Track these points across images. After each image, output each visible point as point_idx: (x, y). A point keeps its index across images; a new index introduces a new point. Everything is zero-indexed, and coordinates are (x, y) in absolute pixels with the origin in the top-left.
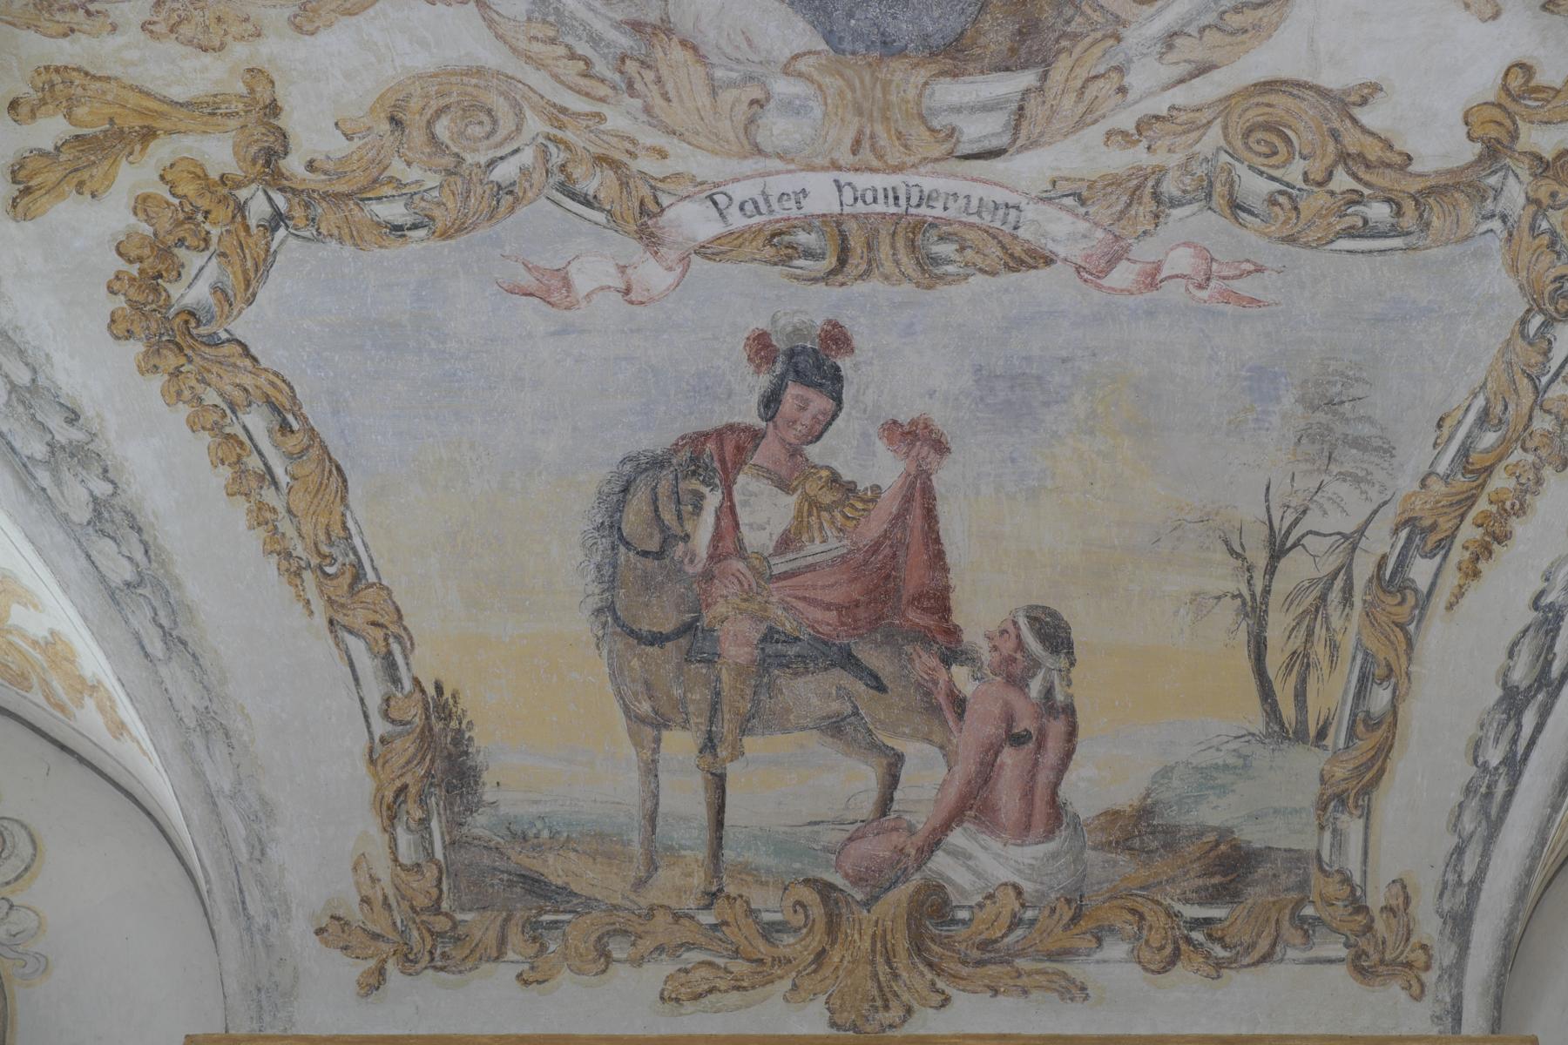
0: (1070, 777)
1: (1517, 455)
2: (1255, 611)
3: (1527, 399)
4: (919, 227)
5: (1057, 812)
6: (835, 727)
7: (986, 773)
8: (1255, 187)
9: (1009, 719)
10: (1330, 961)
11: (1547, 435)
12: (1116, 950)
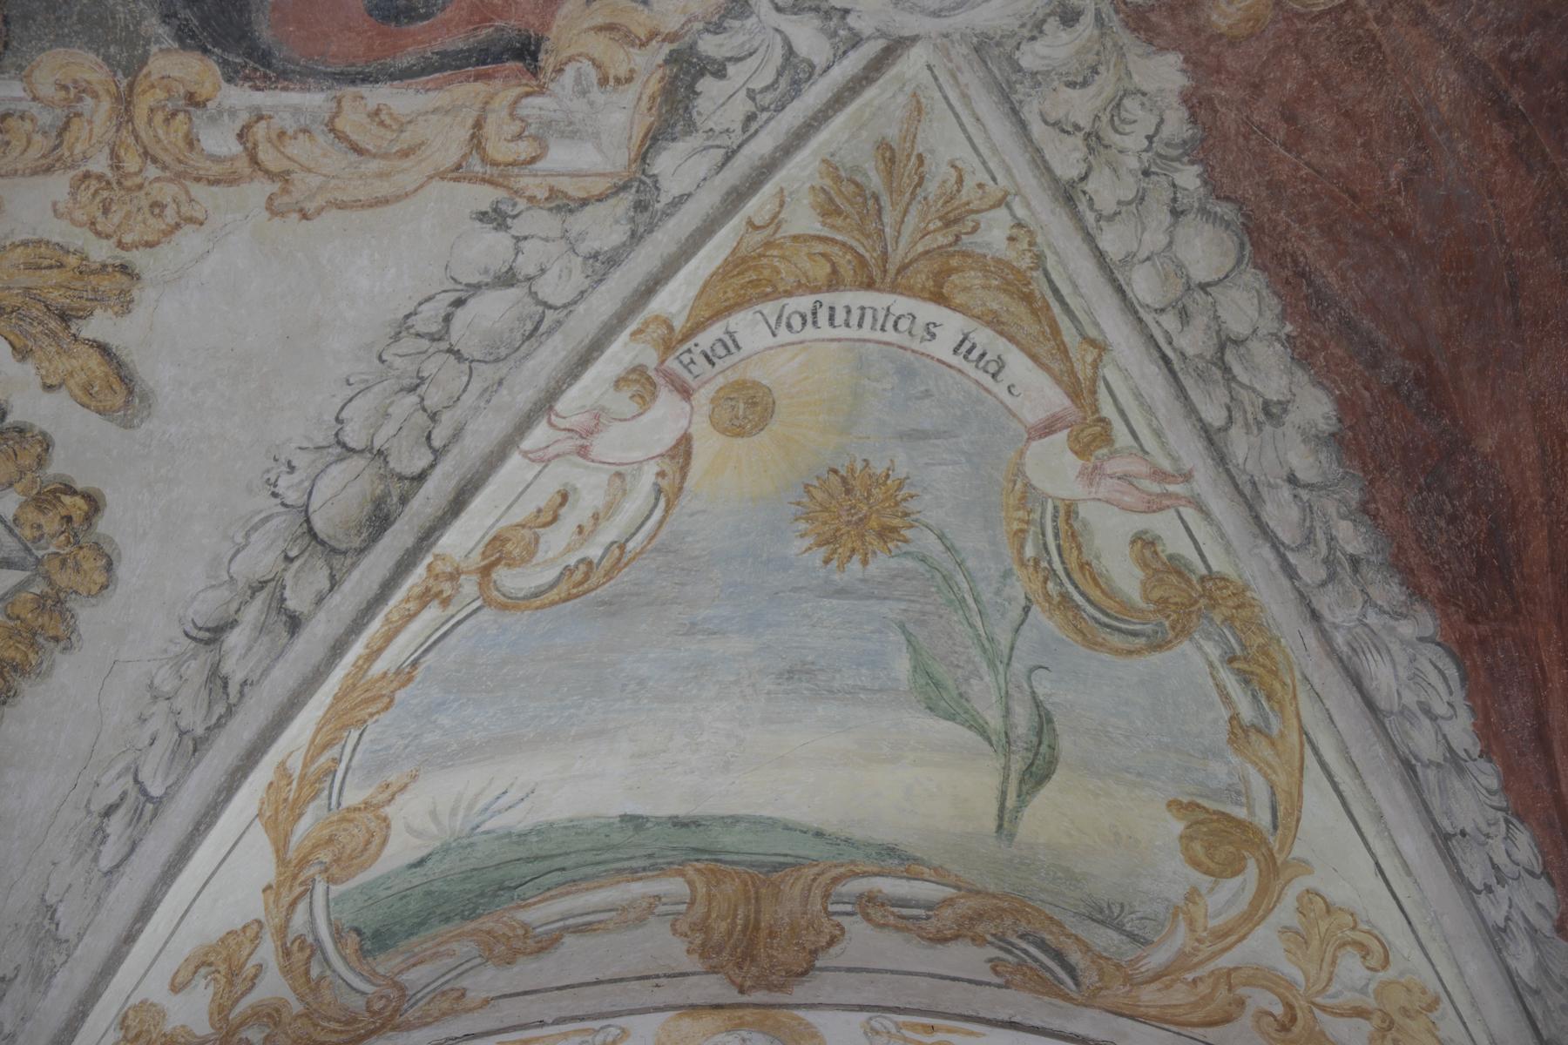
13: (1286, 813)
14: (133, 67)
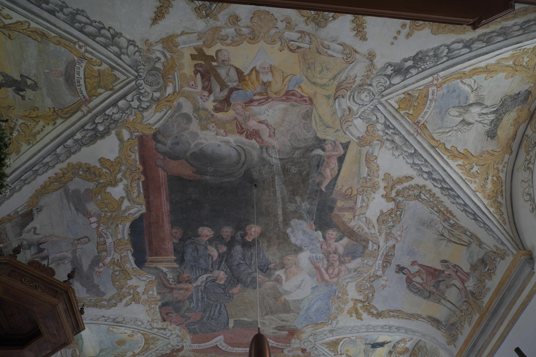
1: (439, 206)
2: (450, 241)
3: (431, 203)
4: (386, 255)
6: (447, 287)
7: (460, 278)
8: (391, 224)
11: (437, 202)
12: (487, 281)
14: (159, 301)
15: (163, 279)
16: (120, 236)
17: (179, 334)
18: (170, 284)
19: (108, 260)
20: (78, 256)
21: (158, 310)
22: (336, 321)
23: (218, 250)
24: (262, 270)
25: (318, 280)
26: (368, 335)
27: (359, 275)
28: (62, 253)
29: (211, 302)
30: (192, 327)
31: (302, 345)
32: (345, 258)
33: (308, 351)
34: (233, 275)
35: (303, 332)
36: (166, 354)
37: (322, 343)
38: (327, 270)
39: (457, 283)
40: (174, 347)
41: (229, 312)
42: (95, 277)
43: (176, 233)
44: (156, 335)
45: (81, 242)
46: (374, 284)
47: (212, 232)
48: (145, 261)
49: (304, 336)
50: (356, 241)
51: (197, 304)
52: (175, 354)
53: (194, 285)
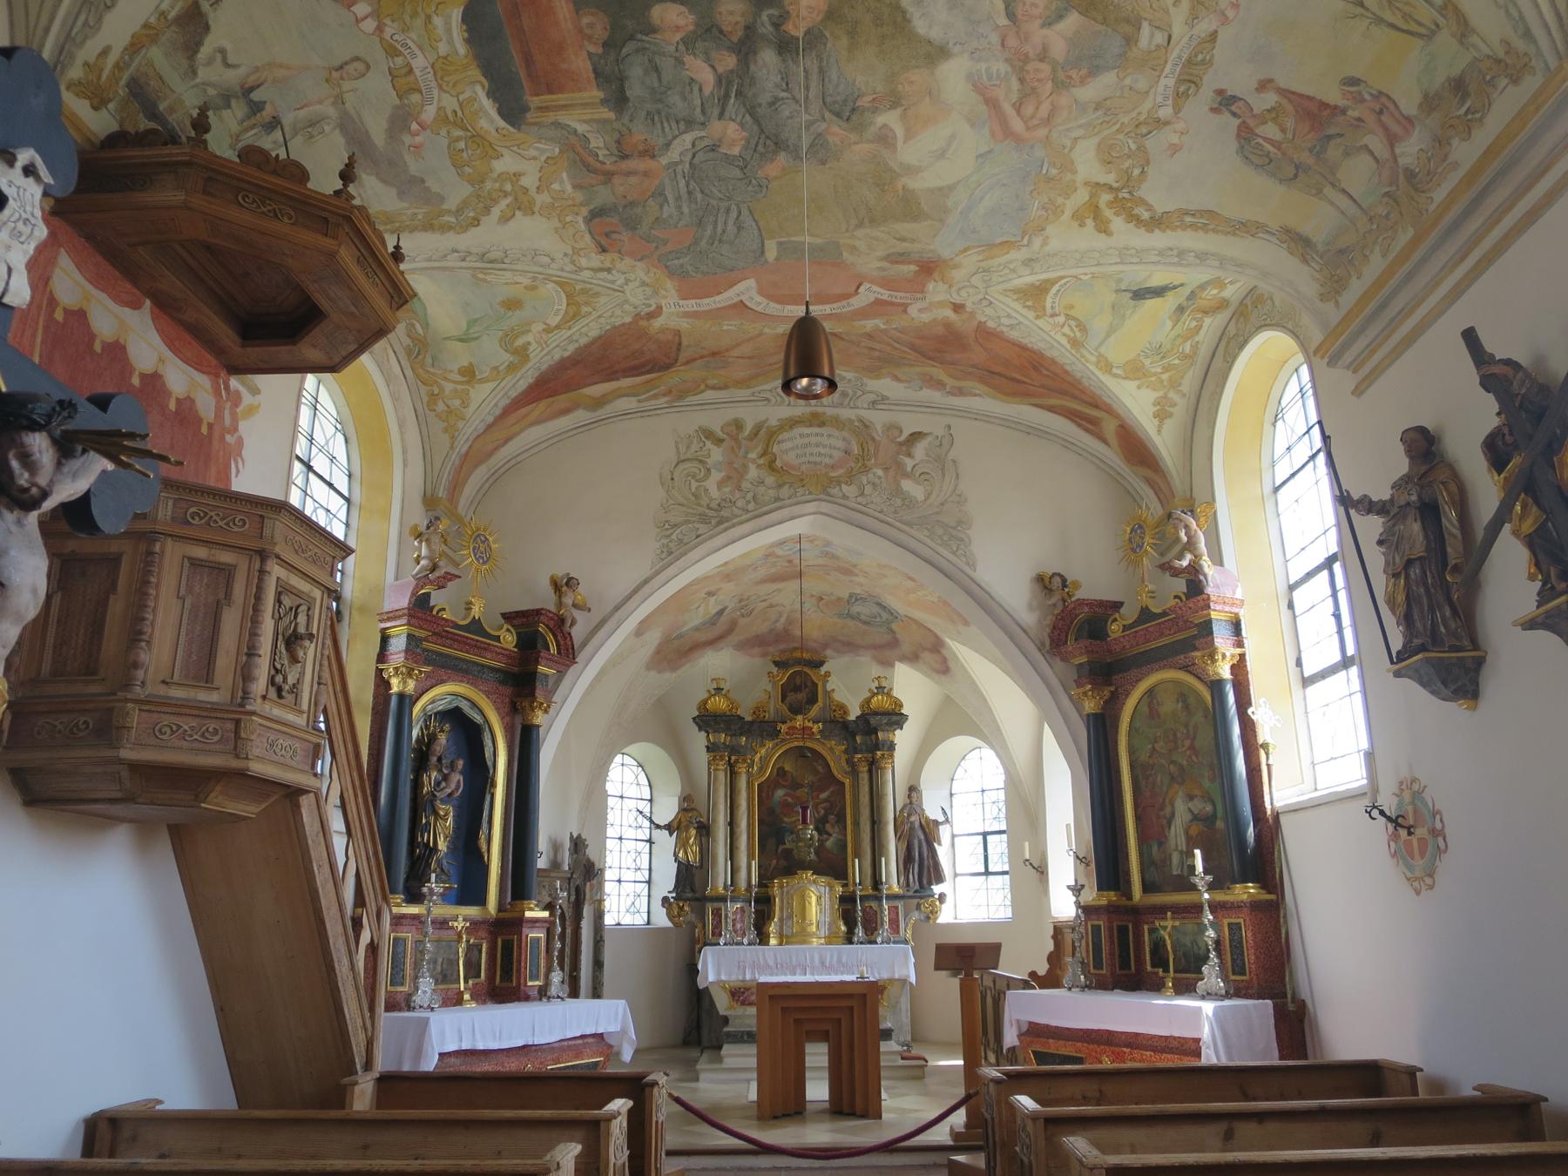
0: (1402, 106)
2: (1379, 21)
4: (1189, 61)
5: (1408, 119)
6: (1347, 154)
7: (1386, 129)
9: (1373, 110)
10: (1505, 88)
12: (1455, 142)
13: (482, 381)
14: (582, 205)
15: (582, 151)
16: (443, 49)
17: (646, 279)
18: (600, 162)
19: (429, 113)
20: (352, 112)
21: (583, 227)
22: (1041, 238)
23: (713, 67)
24: (838, 115)
25: (993, 135)
26: (1123, 272)
27: (1107, 119)
28: (311, 108)
29: (714, 202)
30: (676, 262)
31: (954, 295)
32: (1070, 73)
33: (968, 310)
34: (762, 131)
35: (957, 266)
36: (623, 325)
37: (1005, 290)
38: (1018, 107)
39: (1377, 143)
40: (639, 309)
41: (761, 223)
42: (407, 157)
43: (591, 26)
44: (591, 284)
45: (348, 74)
46: (1150, 143)
47: (692, 18)
48: (526, 109)
49: (958, 275)
50: (1105, 22)
51: (679, 208)
52: (643, 323)
53: (664, 161)
